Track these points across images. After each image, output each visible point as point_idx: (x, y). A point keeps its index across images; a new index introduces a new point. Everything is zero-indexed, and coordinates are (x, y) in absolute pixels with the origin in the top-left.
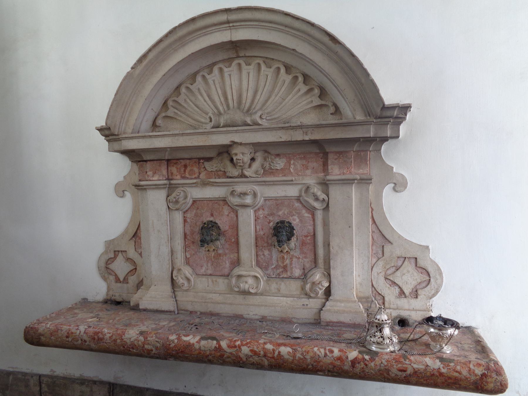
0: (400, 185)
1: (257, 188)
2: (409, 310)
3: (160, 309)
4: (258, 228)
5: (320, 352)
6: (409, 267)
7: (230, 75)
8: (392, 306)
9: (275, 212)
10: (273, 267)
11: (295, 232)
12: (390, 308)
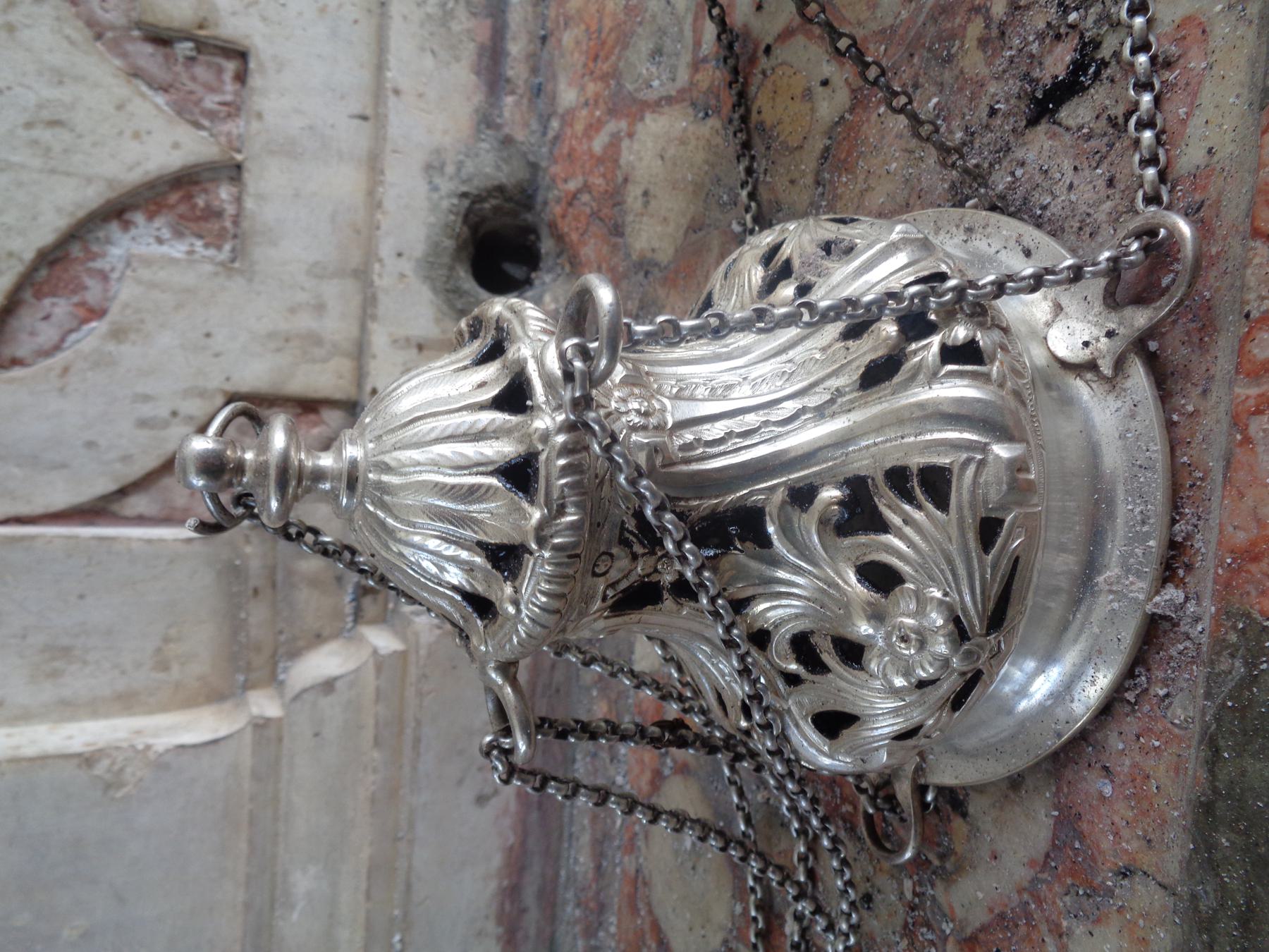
2: (374, 165)
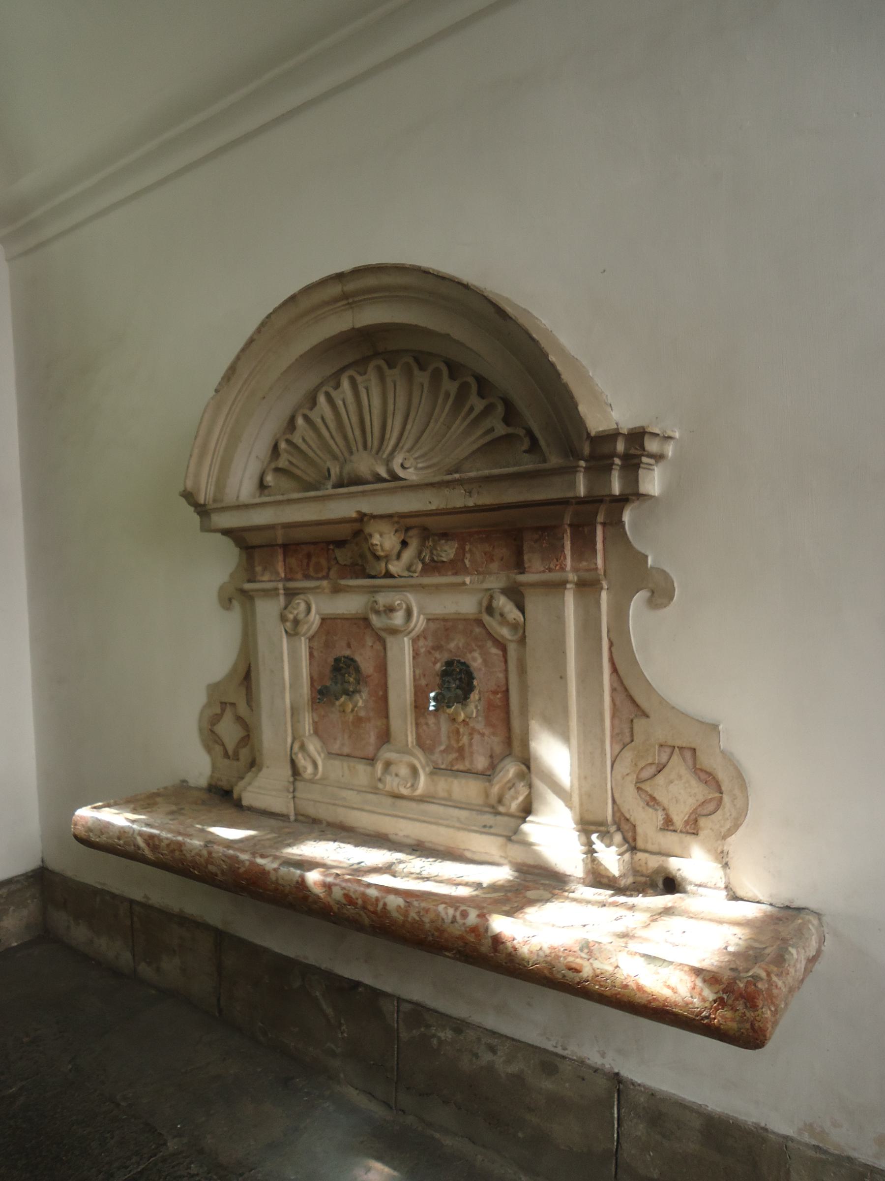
0: (661, 593)
1: (412, 598)
3: (269, 809)
4: (417, 672)
5: (447, 914)
6: (678, 766)
7: (367, 389)
8: (650, 847)
9: (443, 643)
10: (442, 748)
11: (475, 683)
12: (645, 851)
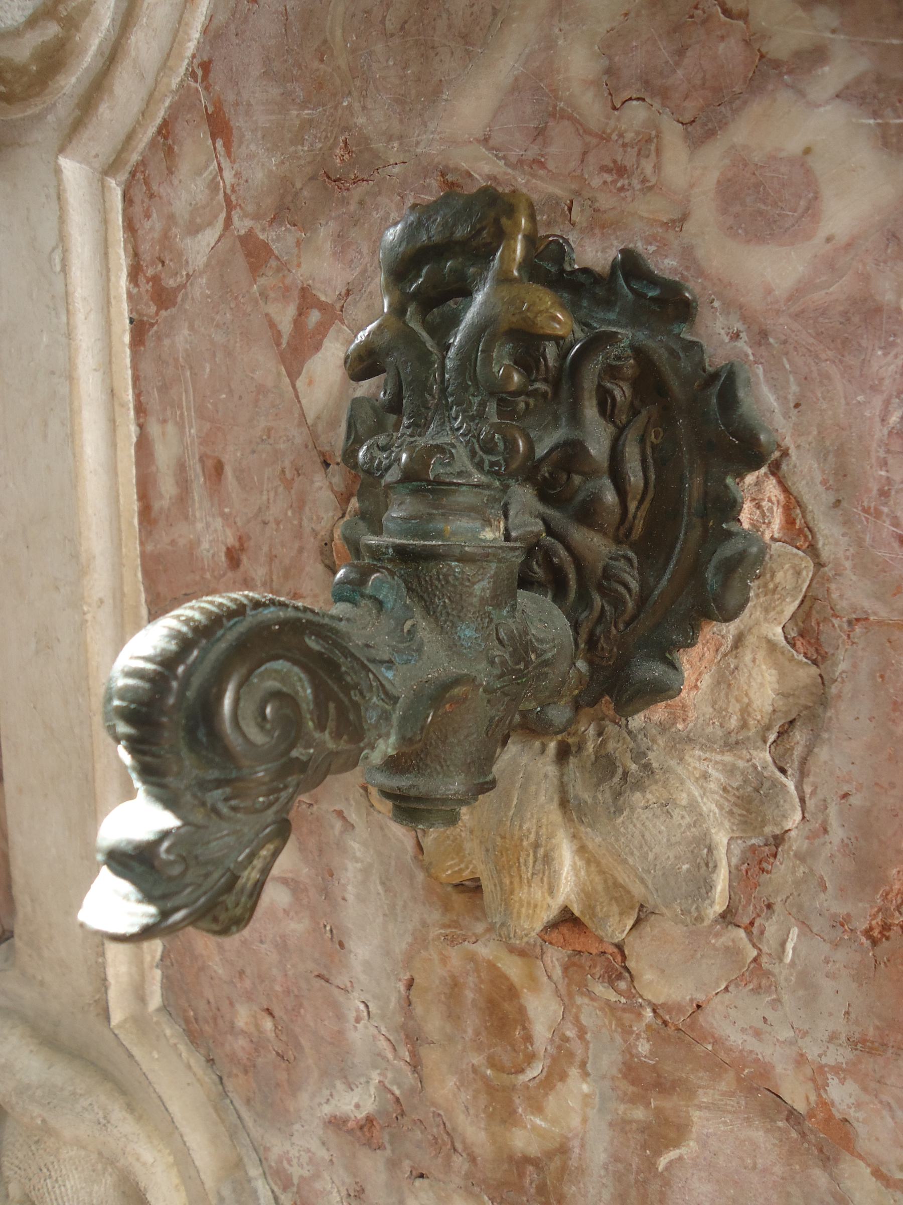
10: (356, 1101)
